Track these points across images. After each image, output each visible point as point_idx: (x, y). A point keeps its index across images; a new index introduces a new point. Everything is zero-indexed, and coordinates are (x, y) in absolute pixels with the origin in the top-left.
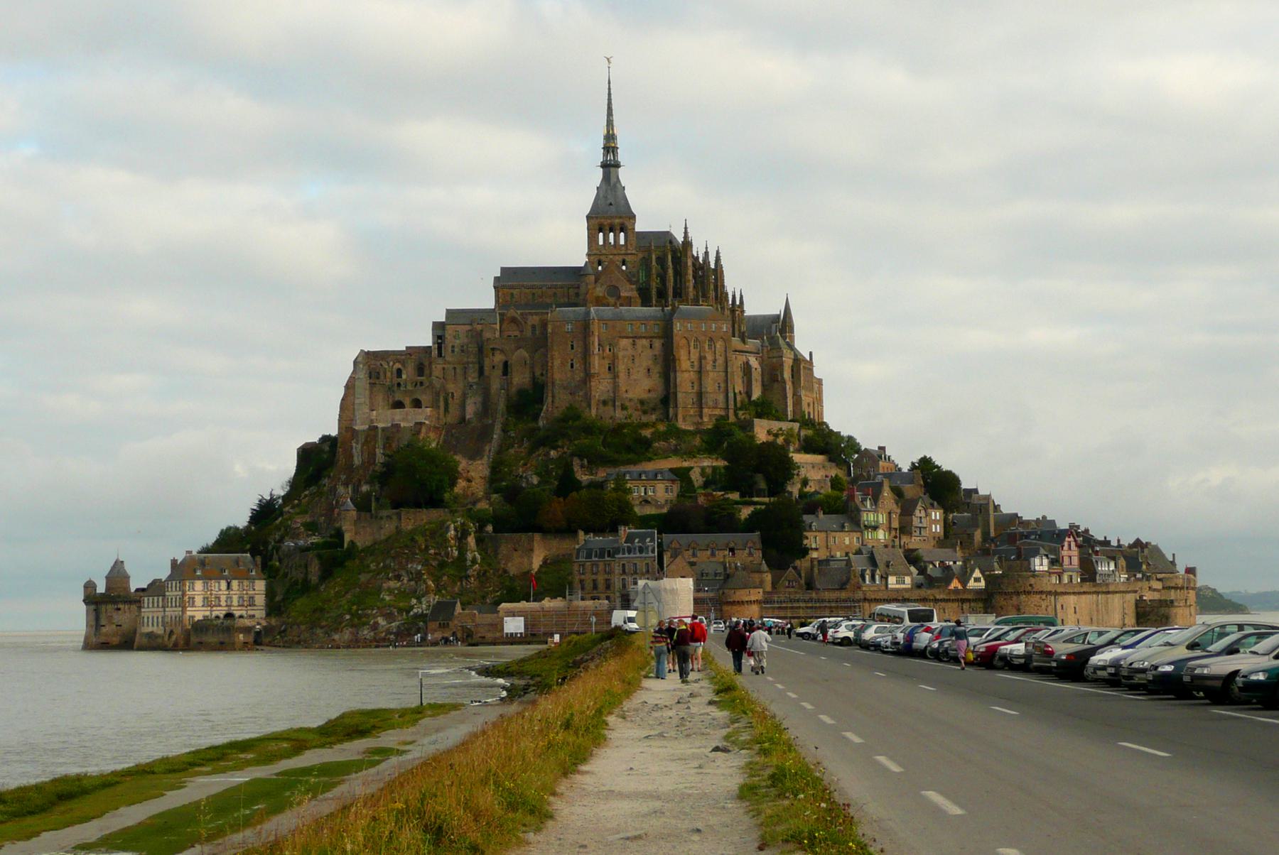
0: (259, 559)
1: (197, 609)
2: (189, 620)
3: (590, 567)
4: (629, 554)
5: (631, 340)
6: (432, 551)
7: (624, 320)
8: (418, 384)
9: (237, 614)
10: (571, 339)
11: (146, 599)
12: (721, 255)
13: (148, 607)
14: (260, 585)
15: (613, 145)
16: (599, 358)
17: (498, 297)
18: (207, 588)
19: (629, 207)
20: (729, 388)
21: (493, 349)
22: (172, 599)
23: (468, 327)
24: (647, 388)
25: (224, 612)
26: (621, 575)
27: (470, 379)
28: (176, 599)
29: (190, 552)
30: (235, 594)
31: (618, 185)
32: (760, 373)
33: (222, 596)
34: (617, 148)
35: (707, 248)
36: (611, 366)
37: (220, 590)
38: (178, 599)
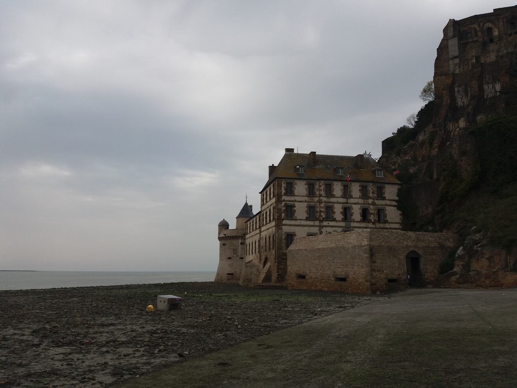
1: (298, 222)
13: (250, 232)
22: (266, 213)
28: (270, 210)
29: (292, 150)
30: (355, 204)
33: (335, 205)
37: (333, 196)
38: (272, 211)
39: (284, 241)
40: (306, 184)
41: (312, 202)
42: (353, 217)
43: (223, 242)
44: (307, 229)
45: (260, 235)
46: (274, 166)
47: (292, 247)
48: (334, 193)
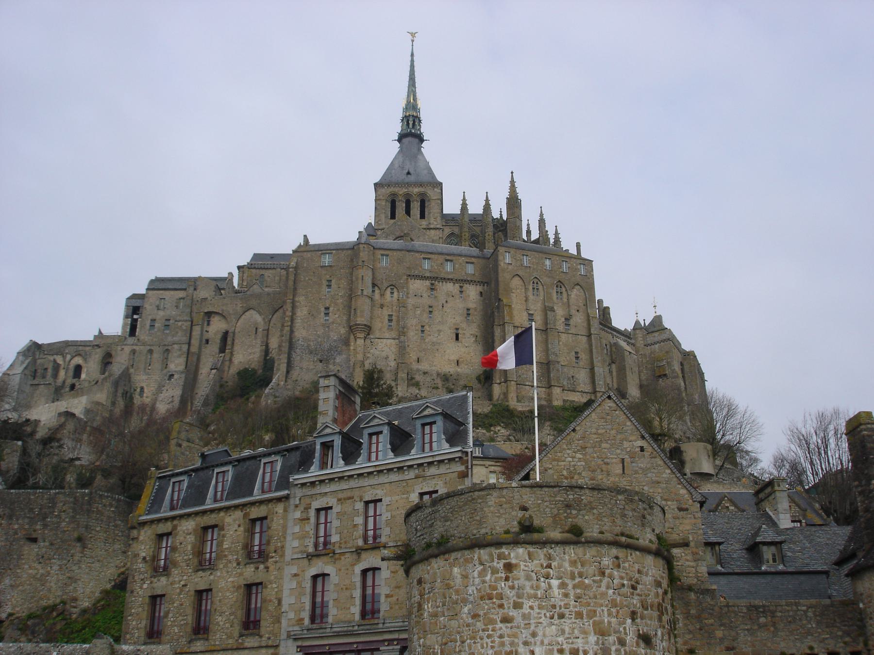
3: (191, 538)
4: (346, 464)
5: (428, 283)
7: (418, 252)
10: (328, 277)
12: (560, 236)
15: (415, 114)
16: (373, 306)
17: (243, 280)
19: (433, 176)
20: (595, 360)
21: (209, 314)
23: (181, 294)
24: (454, 357)
26: (310, 557)
27: (172, 367)
31: (419, 157)
32: (636, 361)
34: (420, 121)
35: (541, 215)
36: (394, 318)
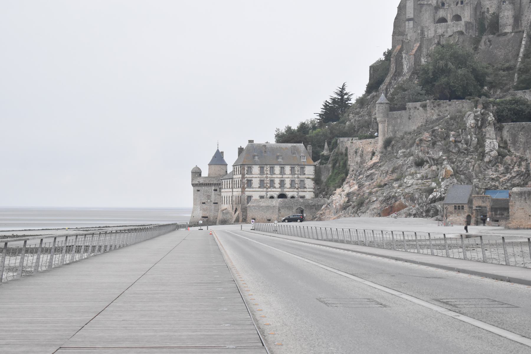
0: (309, 147)
1: (254, 190)
2: (248, 199)
6: (452, 139)
8: (459, 3)
9: (289, 194)
11: (224, 181)
13: (225, 188)
14: (310, 171)
18: (263, 172)
22: (236, 181)
25: (278, 193)
28: (238, 181)
30: (287, 178)
33: (276, 179)
37: (274, 174)
39: (246, 200)
40: (259, 167)
41: (262, 178)
42: (286, 186)
43: (197, 188)
44: (259, 193)
45: (232, 194)
46: (242, 147)
47: (249, 204)
48: (275, 172)
